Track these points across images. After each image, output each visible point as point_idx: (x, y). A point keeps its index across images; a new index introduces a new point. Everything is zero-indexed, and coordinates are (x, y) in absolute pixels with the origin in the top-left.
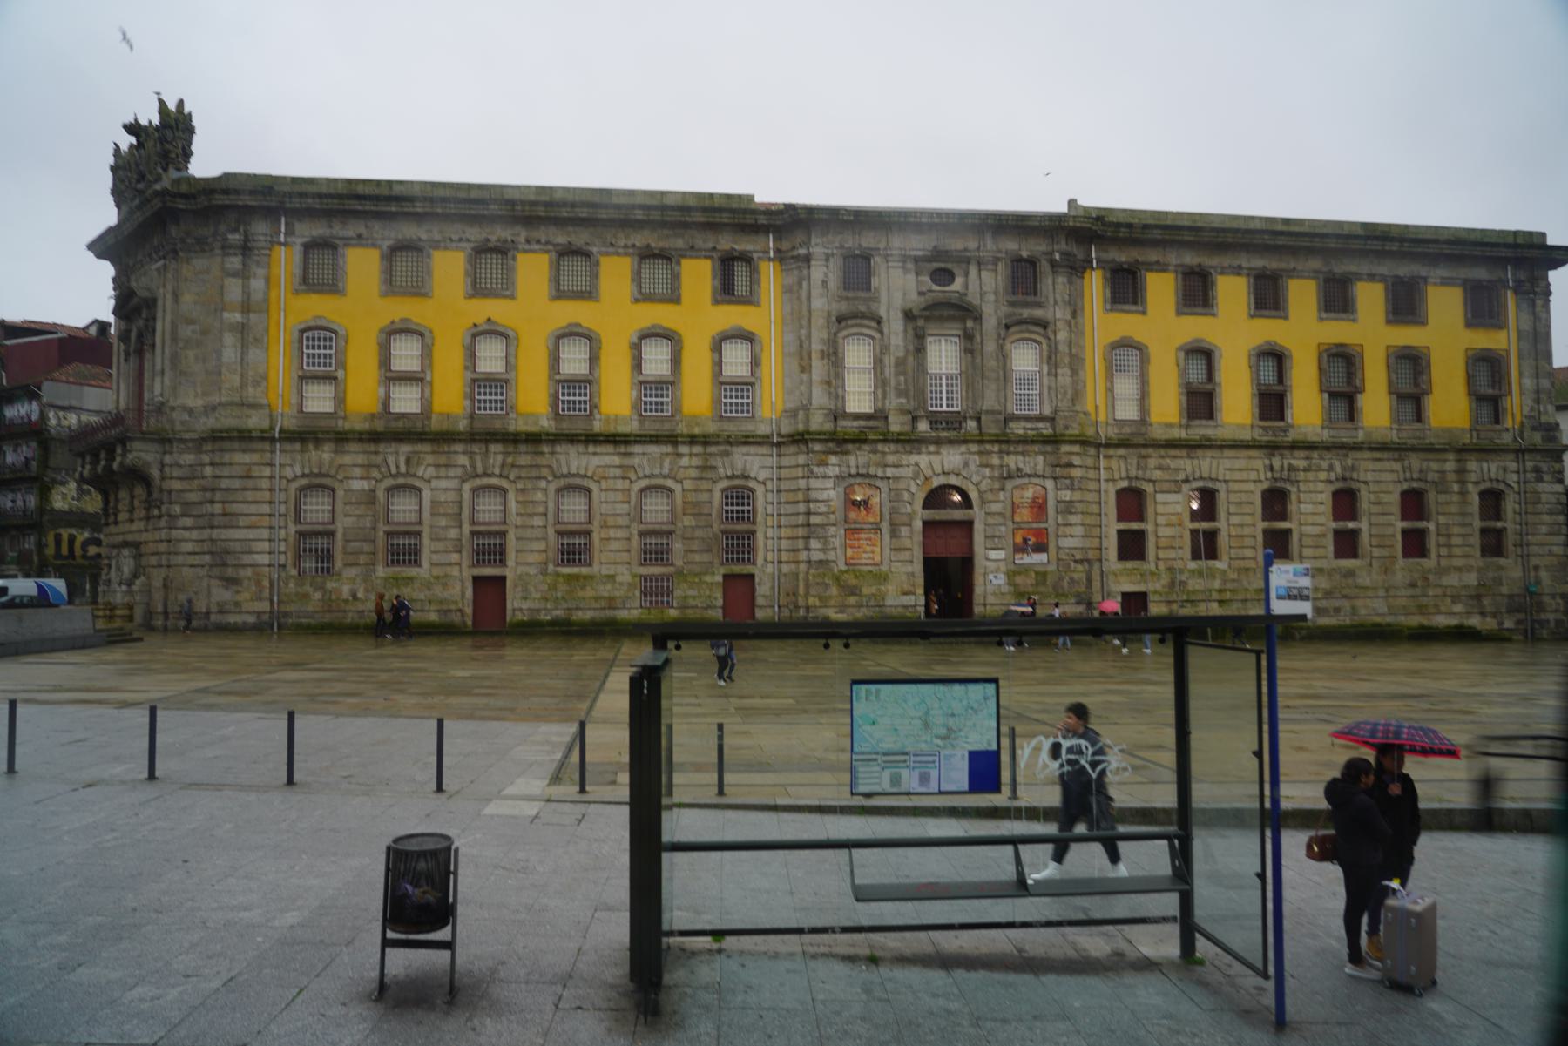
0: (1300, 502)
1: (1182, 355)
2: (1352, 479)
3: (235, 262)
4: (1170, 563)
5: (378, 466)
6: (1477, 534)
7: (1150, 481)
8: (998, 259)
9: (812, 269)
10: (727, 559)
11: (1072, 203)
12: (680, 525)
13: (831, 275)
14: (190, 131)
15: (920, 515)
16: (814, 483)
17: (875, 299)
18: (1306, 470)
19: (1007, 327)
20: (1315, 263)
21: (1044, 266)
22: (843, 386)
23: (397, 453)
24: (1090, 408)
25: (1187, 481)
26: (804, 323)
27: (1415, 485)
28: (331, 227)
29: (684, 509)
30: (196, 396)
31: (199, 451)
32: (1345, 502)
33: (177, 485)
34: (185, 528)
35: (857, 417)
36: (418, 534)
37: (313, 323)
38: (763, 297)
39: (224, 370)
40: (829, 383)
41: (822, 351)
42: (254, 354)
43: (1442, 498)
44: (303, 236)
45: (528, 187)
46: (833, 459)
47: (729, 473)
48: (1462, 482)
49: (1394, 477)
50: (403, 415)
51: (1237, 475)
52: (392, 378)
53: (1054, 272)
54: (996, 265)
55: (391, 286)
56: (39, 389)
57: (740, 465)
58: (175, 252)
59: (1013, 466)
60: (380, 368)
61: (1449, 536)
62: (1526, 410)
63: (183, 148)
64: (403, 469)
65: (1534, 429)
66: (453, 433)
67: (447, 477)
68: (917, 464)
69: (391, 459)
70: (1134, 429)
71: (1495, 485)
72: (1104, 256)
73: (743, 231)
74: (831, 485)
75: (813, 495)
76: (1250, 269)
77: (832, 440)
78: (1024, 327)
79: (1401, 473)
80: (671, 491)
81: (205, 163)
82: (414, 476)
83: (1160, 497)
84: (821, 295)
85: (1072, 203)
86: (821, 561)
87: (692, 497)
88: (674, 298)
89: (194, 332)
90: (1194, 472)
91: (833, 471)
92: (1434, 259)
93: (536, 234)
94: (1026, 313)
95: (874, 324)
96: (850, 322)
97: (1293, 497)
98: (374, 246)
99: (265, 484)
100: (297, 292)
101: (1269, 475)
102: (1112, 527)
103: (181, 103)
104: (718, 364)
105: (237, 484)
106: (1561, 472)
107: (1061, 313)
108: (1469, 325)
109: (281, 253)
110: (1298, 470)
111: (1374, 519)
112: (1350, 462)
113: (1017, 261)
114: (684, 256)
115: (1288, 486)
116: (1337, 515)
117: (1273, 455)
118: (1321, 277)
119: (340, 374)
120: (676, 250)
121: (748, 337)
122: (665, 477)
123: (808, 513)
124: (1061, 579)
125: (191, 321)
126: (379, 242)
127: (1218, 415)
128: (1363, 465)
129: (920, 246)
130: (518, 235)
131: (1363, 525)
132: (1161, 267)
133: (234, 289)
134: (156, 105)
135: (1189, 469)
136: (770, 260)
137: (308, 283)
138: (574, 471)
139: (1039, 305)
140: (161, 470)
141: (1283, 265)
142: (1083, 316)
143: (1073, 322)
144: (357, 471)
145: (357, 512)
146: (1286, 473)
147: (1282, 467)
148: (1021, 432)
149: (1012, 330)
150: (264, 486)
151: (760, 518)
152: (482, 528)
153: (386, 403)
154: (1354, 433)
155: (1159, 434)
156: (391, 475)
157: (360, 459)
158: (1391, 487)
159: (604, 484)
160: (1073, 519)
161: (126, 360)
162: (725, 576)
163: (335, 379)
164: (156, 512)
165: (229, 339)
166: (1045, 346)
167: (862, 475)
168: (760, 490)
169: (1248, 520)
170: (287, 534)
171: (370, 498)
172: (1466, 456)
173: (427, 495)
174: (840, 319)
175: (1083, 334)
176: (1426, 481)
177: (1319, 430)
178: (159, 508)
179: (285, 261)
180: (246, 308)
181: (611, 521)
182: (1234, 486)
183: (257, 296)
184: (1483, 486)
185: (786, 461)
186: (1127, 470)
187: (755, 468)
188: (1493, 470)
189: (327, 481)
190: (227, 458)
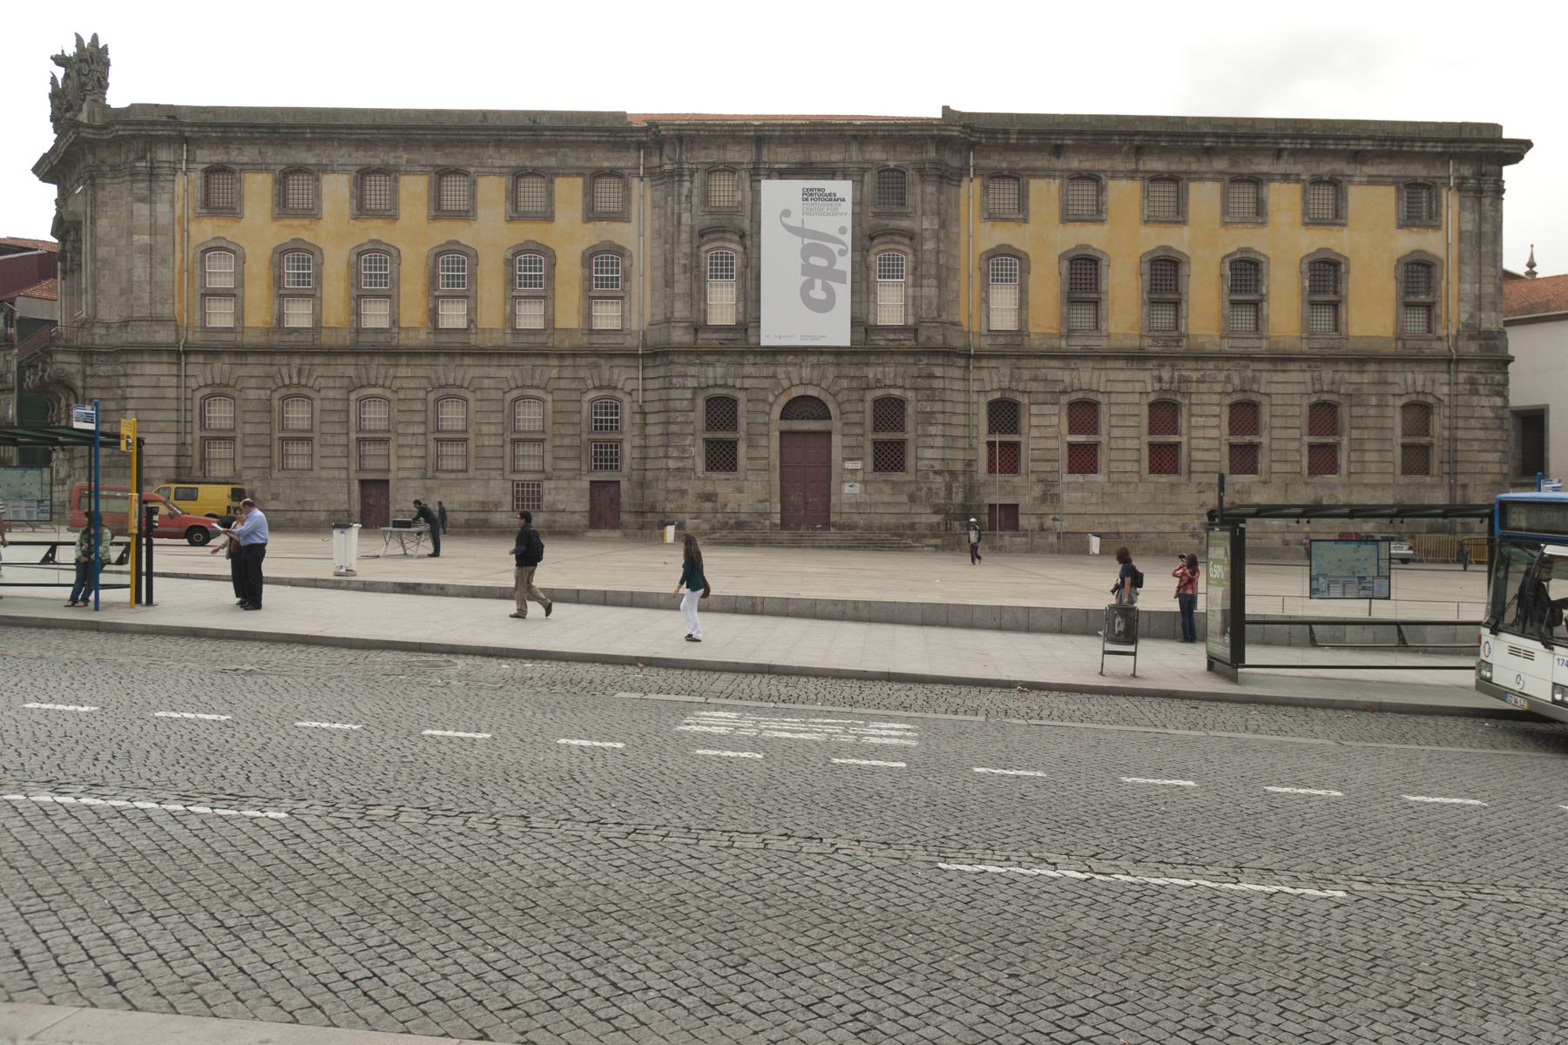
0: (1191, 415)
1: (1066, 264)
2: (1251, 391)
3: (141, 187)
4: (1043, 476)
6: (1398, 450)
7: (1024, 392)
8: (864, 170)
10: (596, 466)
11: (946, 109)
13: (695, 191)
14: (107, 64)
15: (777, 425)
16: (674, 394)
19: (872, 239)
20: (1220, 164)
21: (912, 176)
22: (705, 300)
23: (289, 365)
24: (963, 319)
25: (1064, 392)
27: (1326, 397)
28: (228, 153)
32: (1245, 414)
35: (719, 329)
37: (213, 244)
43: (1357, 411)
46: (692, 370)
48: (1382, 395)
49: (1302, 389)
50: (296, 330)
51: (1120, 387)
52: (282, 295)
53: (923, 182)
54: (863, 176)
55: (283, 207)
56: (12, 304)
59: (871, 376)
61: (1364, 451)
62: (1464, 317)
63: (99, 80)
64: (295, 381)
65: (1471, 338)
68: (774, 376)
69: (284, 370)
70: (1009, 340)
71: (1421, 398)
72: (983, 163)
75: (672, 404)
76: (1146, 172)
78: (889, 238)
79: (1310, 385)
80: (544, 401)
81: (117, 97)
82: (305, 386)
83: (1034, 410)
85: (946, 110)
86: (678, 469)
88: (548, 217)
90: (1072, 383)
91: (691, 382)
92: (1358, 157)
93: (416, 156)
94: (895, 223)
96: (712, 236)
97: (1184, 411)
98: (267, 170)
101: (1157, 386)
102: (983, 436)
103: (95, 38)
106: (1505, 384)
107: (928, 224)
108: (1402, 225)
109: (180, 180)
111: (1277, 433)
112: (1249, 374)
113: (883, 171)
114: (557, 175)
115: (1179, 398)
116: (1234, 429)
117: (1163, 366)
118: (1227, 178)
120: (549, 168)
122: (537, 387)
123: (668, 423)
124: (919, 489)
127: (1103, 326)
128: (1265, 376)
129: (786, 159)
131: (1264, 439)
132: (1047, 174)
135: (1067, 380)
137: (209, 207)
138: (451, 381)
139: (906, 216)
140: (84, 381)
141: (1183, 167)
142: (958, 226)
143: (942, 234)
146: (1175, 384)
148: (883, 343)
149: (875, 242)
151: (626, 428)
152: (367, 435)
153: (280, 317)
154: (1257, 343)
155: (1035, 343)
156: (285, 386)
157: (258, 371)
158: (1297, 400)
159: (479, 395)
160: (933, 430)
161: (63, 278)
162: (591, 482)
166: (910, 257)
167: (721, 386)
168: (627, 399)
169: (1131, 432)
170: (193, 440)
172: (1389, 367)
173: (317, 404)
175: (957, 243)
176: (1338, 393)
177: (1218, 340)
179: (185, 187)
180: (153, 230)
181: (485, 429)
182: (1114, 398)
184: (1404, 400)
185: (650, 373)
186: (999, 382)
188: (1420, 382)
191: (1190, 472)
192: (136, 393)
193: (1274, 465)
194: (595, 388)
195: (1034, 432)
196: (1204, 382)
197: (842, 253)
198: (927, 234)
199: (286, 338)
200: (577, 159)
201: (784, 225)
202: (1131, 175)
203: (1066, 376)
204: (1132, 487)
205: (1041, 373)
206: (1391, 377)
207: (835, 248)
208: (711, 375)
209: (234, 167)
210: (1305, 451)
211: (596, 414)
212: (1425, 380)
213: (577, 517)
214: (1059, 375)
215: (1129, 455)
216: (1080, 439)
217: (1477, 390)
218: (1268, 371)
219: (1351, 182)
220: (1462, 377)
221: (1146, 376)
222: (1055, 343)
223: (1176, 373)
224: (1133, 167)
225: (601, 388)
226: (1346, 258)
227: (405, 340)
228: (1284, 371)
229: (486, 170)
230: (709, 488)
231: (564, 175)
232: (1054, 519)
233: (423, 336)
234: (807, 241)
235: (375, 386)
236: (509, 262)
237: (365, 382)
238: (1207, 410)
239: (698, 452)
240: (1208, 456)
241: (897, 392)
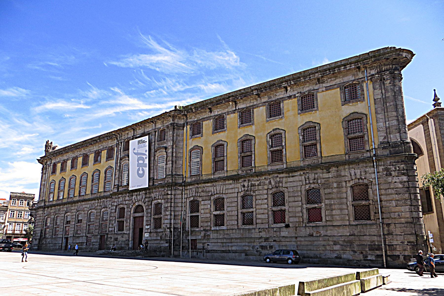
4: (205, 228)
6: (351, 208)
18: (258, 185)
25: (212, 195)
27: (313, 186)
43: (327, 191)
48: (339, 183)
61: (332, 210)
65: (384, 148)
83: (202, 203)
91: (115, 204)
101: (243, 189)
110: (256, 186)
111: (291, 204)
112: (278, 179)
118: (267, 104)
124: (163, 234)
128: (284, 180)
132: (208, 118)
147: (248, 185)
172: (341, 168)
184: (352, 183)
191: (257, 224)
193: (291, 218)
195: (202, 211)
196: (260, 185)
197: (146, 158)
198: (169, 147)
201: (134, 153)
202: (234, 112)
203: (212, 189)
204: (234, 231)
205: (204, 189)
206: (343, 174)
207: (144, 157)
208: (119, 201)
210: (305, 211)
212: (361, 172)
213: (97, 246)
214: (212, 189)
215: (233, 218)
216: (218, 213)
217: (391, 175)
218: (286, 177)
219: (318, 92)
220: (381, 168)
221: (239, 185)
222: (210, 177)
223: (250, 183)
224: (234, 109)
225: (104, 208)
226: (318, 123)
228: (293, 176)
232: (208, 245)
234: (139, 156)
236: (93, 176)
238: (262, 197)
239: (116, 224)
240: (263, 216)
241: (159, 201)
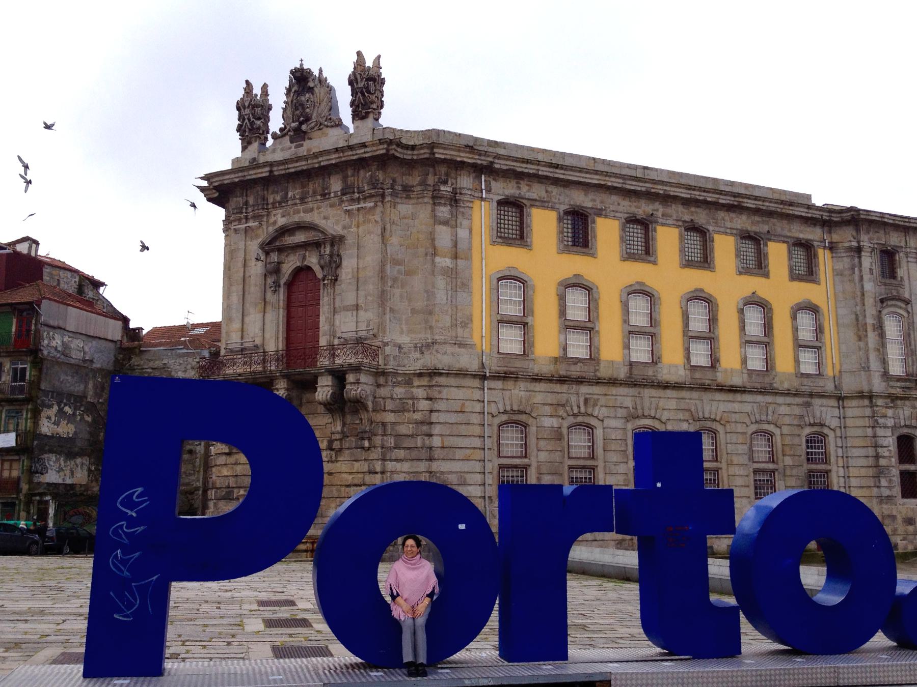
3: (444, 211)
5: (563, 405)
9: (863, 258)
12: (781, 465)
16: (880, 432)
17: (901, 285)
26: (858, 299)
28: (519, 188)
29: (783, 451)
30: (402, 332)
31: (409, 383)
33: (390, 417)
34: (396, 460)
36: (593, 469)
37: (508, 273)
38: (822, 276)
39: (437, 309)
40: (878, 350)
41: (874, 325)
42: (461, 296)
44: (499, 195)
45: (662, 171)
46: (890, 412)
47: (812, 422)
52: (568, 326)
57: (818, 414)
58: (383, 196)
60: (560, 317)
66: (616, 379)
67: (615, 417)
69: (573, 399)
73: (806, 223)
74: (890, 434)
77: (889, 397)
80: (771, 435)
84: (870, 280)
87: (788, 440)
89: (399, 272)
91: (890, 422)
95: (903, 305)
96: (890, 303)
98: (553, 208)
99: (476, 419)
100: (494, 243)
104: (795, 330)
105: (453, 418)
114: (770, 240)
119: (529, 320)
121: (813, 309)
122: (769, 423)
125: (396, 262)
126: (557, 206)
130: (657, 210)
133: (444, 236)
134: (355, 58)
136: (825, 248)
138: (707, 415)
144: (548, 410)
145: (549, 448)
150: (475, 422)
151: (833, 459)
153: (565, 349)
163: (525, 324)
164: (366, 444)
165: (441, 282)
167: (906, 426)
168: (831, 435)
171: (558, 436)
173: (599, 433)
174: (882, 301)
178: (369, 439)
181: (736, 460)
183: (462, 246)
187: (828, 417)
189: (523, 418)
190: (445, 393)
192: (442, 418)
194: (810, 425)
199: (573, 368)
200: (782, 229)
208: (902, 417)
209: (524, 201)
211: (808, 448)
227: (665, 375)
229: (722, 230)
230: (910, 514)
231: (775, 241)
233: (682, 372)
235: (646, 417)
237: (640, 412)
